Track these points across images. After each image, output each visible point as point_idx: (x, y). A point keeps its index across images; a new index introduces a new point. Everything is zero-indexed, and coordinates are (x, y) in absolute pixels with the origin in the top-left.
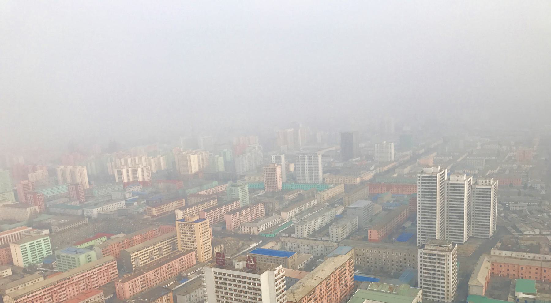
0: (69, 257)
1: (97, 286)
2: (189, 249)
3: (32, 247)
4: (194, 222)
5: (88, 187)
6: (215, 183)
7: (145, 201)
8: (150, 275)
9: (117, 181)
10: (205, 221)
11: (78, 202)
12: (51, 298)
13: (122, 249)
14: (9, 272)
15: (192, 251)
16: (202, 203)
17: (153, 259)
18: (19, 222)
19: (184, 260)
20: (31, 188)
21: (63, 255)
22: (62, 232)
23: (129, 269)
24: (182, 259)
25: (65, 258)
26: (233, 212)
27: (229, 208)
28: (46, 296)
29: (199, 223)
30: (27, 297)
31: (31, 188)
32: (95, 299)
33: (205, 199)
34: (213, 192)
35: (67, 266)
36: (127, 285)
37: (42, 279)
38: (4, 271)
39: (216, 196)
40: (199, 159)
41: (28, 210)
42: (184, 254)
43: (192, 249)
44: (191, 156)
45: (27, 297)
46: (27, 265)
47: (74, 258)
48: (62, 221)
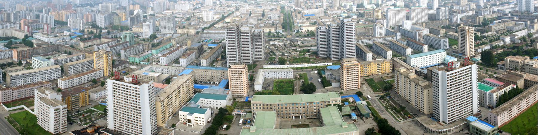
9: (68, 26)
15: (101, 69)
42: (96, 70)
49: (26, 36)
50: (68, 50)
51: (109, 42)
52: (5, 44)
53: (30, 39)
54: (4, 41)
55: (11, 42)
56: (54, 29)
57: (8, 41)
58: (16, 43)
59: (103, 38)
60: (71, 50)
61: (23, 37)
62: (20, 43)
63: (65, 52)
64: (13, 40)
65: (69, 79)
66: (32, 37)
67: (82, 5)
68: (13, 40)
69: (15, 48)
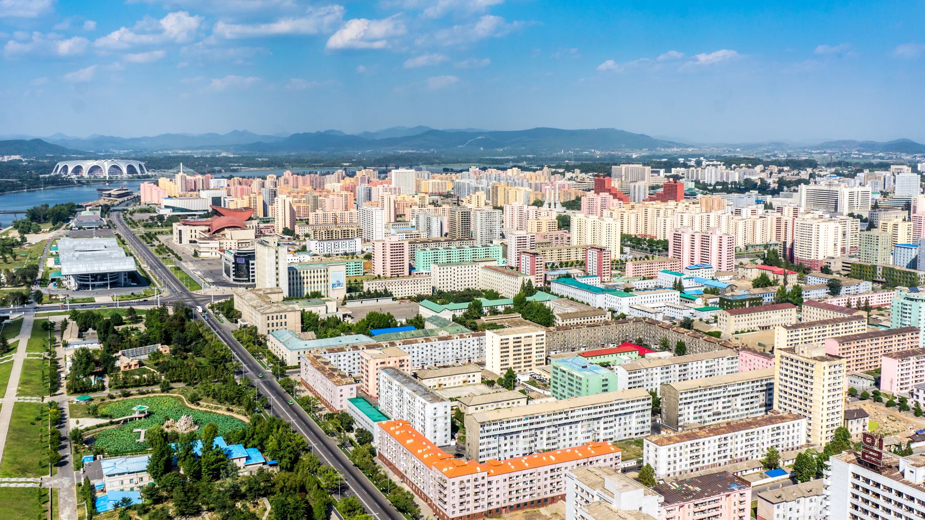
0: (572, 375)
1: (611, 439)
2: (795, 412)
3: (518, 341)
4: (815, 359)
5: (618, 257)
6: (866, 286)
7: (718, 300)
8: (709, 446)
10: (837, 362)
11: (598, 279)
12: (533, 438)
13: (664, 381)
14: (478, 377)
16: (835, 321)
17: (719, 414)
18: (502, 298)
19: (781, 431)
20: (528, 245)
21: (565, 369)
22: (566, 328)
23: (673, 424)
24: (778, 428)
25: (566, 375)
26: (903, 355)
27: (896, 344)
28: (528, 433)
29: (826, 364)
30: (498, 426)
31: (528, 245)
32: (605, 461)
33: (840, 315)
34: (859, 303)
35: (566, 391)
36: (663, 451)
37: (523, 402)
38: (471, 375)
39: (864, 314)
40: (836, 234)
41: (520, 279)
42: (783, 419)
43: (802, 412)
44: (822, 225)
45: (498, 426)
46: (505, 372)
47: (581, 379)
48: (570, 310)
49: (529, 290)
50: (673, 338)
51: (835, 321)
52: (459, 314)
53: (539, 297)
54: (452, 305)
55: (478, 306)
56: (620, 266)
57: (466, 305)
58: (494, 312)
59: (811, 303)
60: (686, 337)
61: (518, 290)
62: (508, 311)
63: (665, 346)
64: (486, 303)
65: (682, 438)
66: (548, 290)
67: (724, 184)
68: (486, 303)
69: (493, 327)
